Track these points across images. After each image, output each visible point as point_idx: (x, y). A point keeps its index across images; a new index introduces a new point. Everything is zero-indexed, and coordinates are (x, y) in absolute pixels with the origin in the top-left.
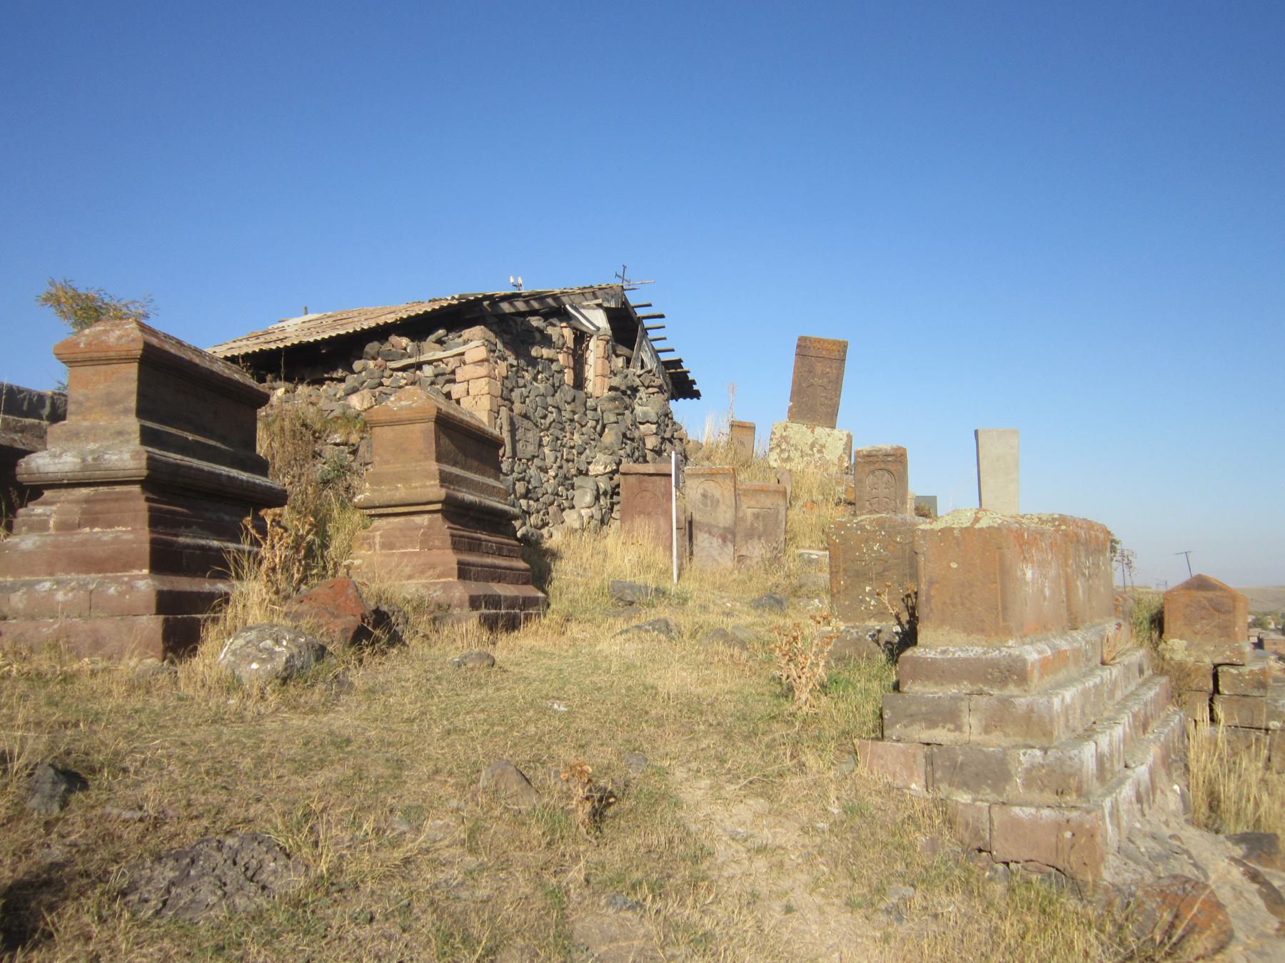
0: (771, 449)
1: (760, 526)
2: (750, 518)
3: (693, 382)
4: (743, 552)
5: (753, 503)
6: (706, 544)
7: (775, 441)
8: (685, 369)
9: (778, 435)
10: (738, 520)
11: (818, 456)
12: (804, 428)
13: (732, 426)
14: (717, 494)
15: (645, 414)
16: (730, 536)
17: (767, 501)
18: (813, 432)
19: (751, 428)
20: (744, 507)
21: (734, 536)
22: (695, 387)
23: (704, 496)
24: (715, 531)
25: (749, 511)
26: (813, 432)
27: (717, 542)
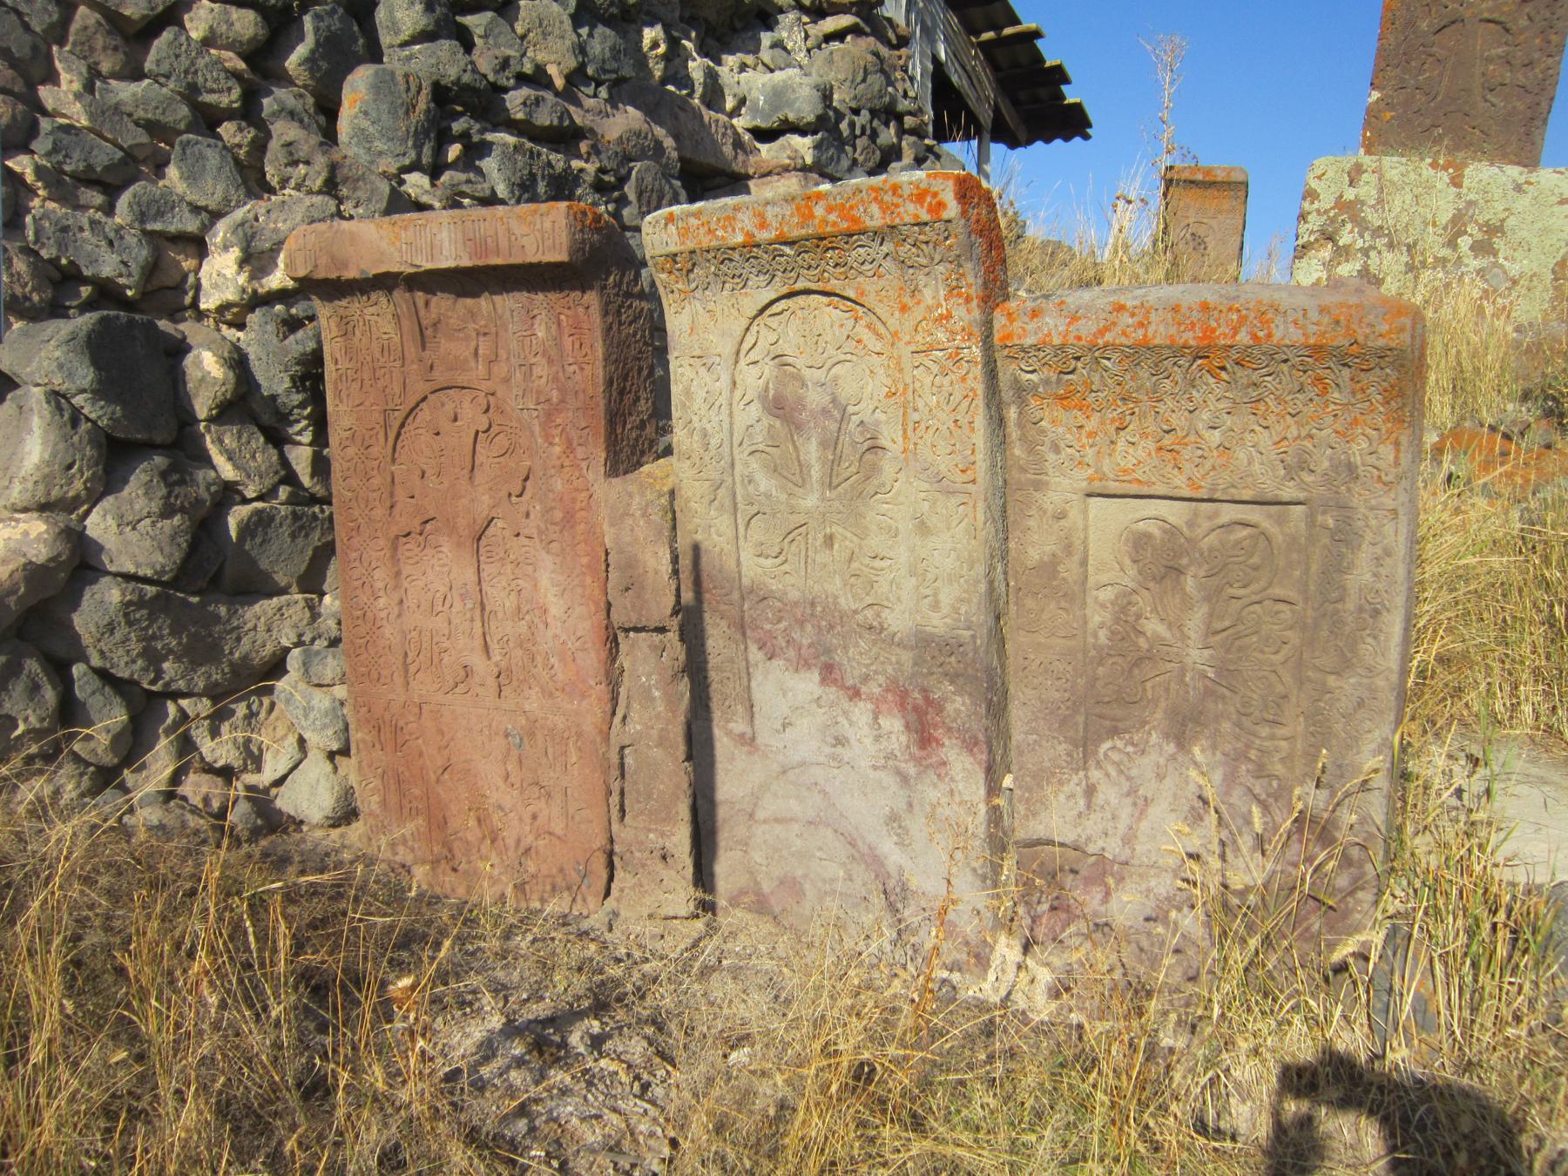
0: (1302, 250)
1: (1186, 638)
2: (1108, 573)
3: (1059, 76)
4: (1056, 818)
5: (1132, 455)
6: (804, 741)
7: (1315, 222)
8: (1028, 24)
9: (1326, 201)
10: (1004, 588)
11: (1474, 263)
12: (1428, 172)
13: (1169, 183)
14: (864, 385)
15: (778, 95)
16: (959, 705)
17: (1249, 445)
18: (1456, 182)
19: (1237, 188)
20: (1063, 485)
21: (996, 707)
22: (1071, 95)
23: (781, 407)
24: (856, 658)
25: (1106, 525)
26: (1456, 182)
27: (872, 733)
